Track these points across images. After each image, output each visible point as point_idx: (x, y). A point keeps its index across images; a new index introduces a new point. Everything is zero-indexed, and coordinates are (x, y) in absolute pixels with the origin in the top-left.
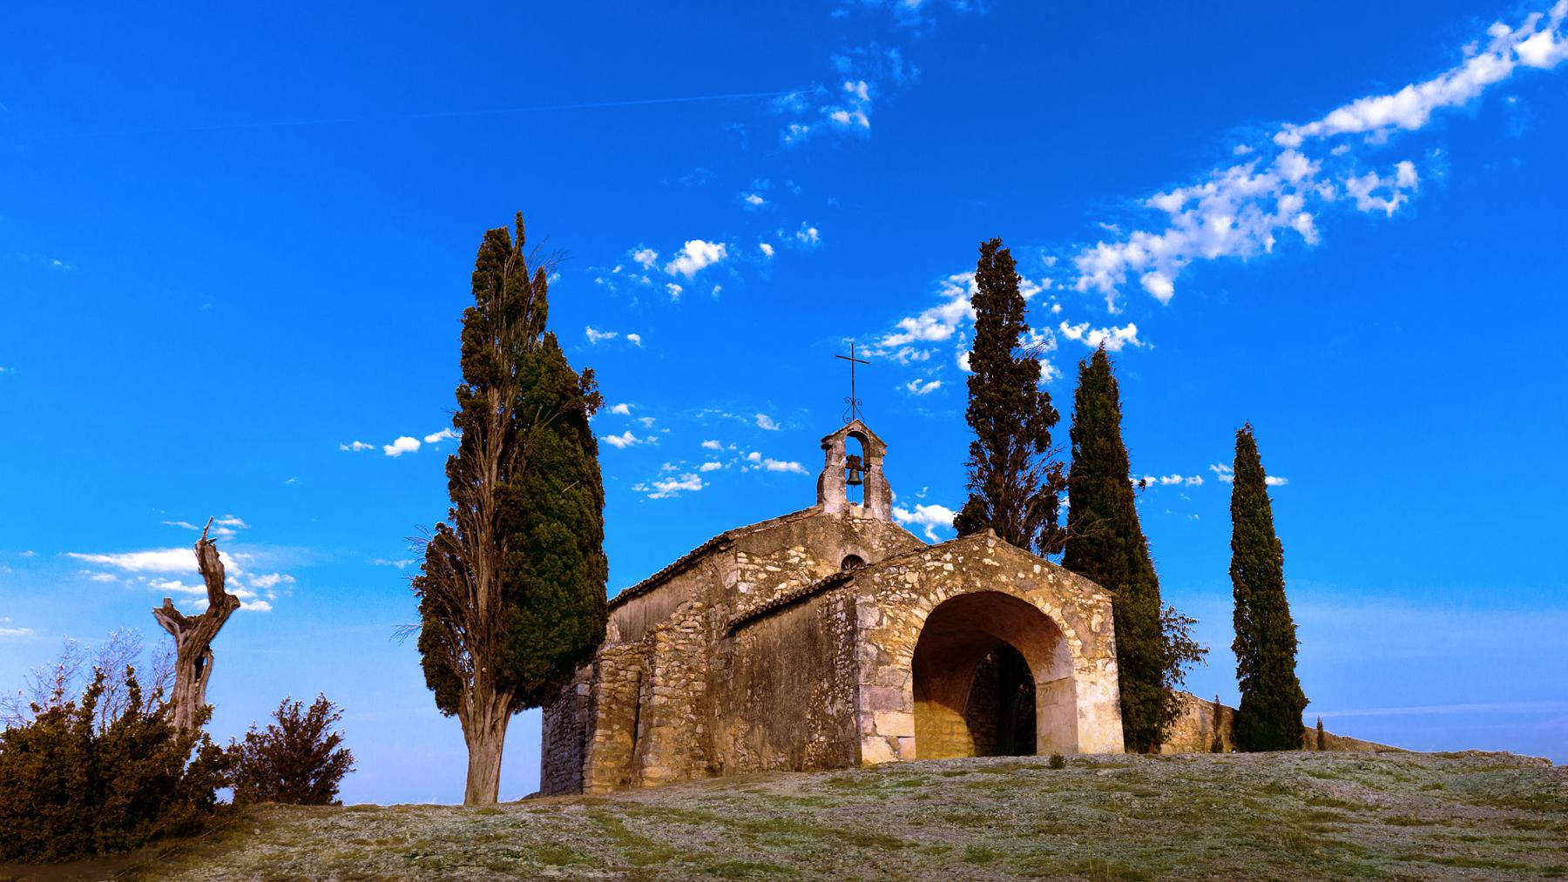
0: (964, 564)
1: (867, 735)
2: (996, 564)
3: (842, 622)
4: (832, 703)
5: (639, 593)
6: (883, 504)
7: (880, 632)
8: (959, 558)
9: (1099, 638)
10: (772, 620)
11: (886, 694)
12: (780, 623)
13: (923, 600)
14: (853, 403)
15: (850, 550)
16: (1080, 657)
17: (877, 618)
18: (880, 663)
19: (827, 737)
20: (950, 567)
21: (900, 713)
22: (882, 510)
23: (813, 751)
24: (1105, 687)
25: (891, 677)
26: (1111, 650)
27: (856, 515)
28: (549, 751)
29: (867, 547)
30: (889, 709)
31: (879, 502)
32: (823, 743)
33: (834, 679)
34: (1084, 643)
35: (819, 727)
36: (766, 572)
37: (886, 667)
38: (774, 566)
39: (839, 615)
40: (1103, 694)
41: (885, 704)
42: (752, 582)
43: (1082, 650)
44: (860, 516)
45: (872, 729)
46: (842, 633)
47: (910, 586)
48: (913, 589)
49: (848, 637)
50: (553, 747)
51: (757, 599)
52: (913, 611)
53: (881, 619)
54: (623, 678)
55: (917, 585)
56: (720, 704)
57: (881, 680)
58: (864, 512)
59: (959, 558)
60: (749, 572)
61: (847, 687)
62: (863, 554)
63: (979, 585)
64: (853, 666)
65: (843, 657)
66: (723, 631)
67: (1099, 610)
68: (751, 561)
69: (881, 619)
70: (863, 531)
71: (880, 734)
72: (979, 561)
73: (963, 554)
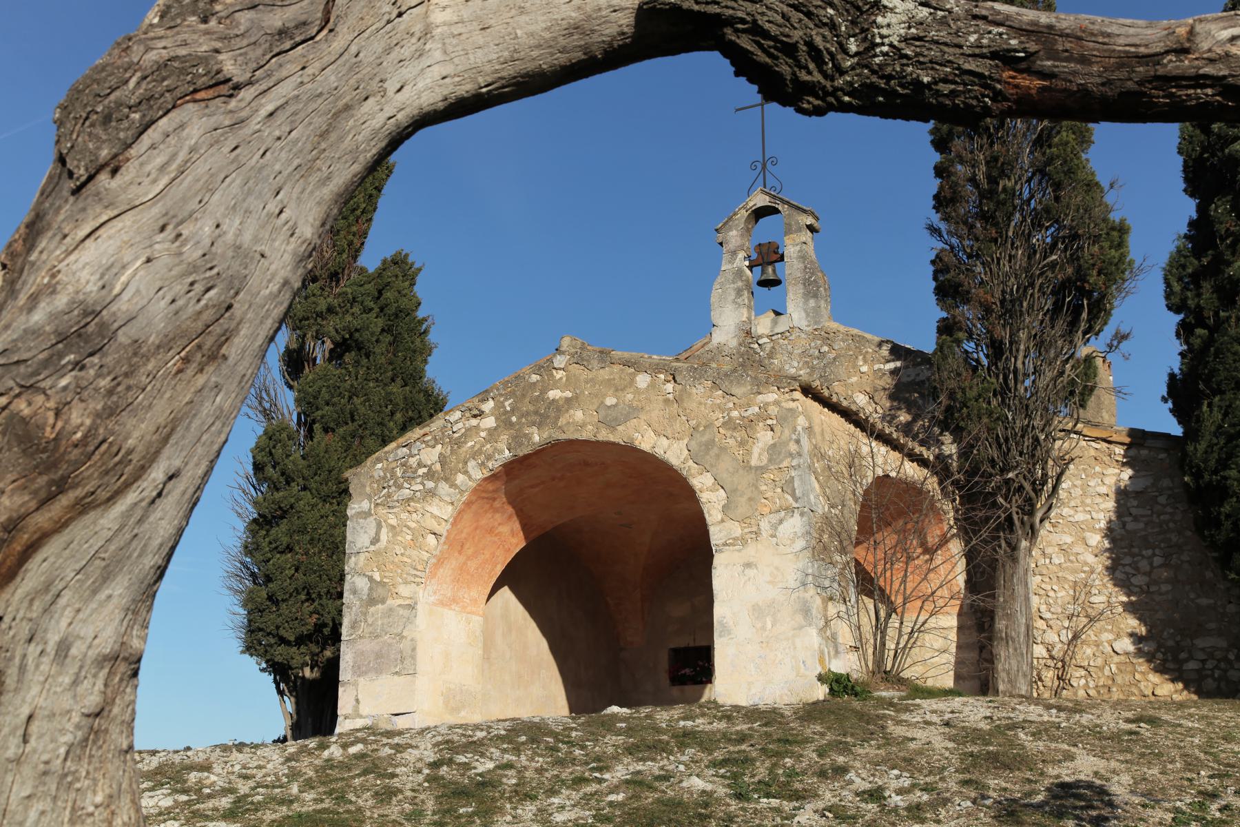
2: (569, 394)
6: (806, 301)
7: (377, 553)
8: (507, 404)
11: (377, 648)
13: (444, 488)
16: (723, 521)
17: (372, 533)
18: (372, 601)
21: (396, 677)
22: (805, 311)
24: (777, 568)
25: (386, 621)
30: (379, 671)
31: (800, 301)
34: (731, 494)
37: (380, 606)
40: (769, 582)
43: (725, 509)
47: (425, 470)
48: (430, 475)
52: (428, 508)
58: (775, 323)
59: (507, 404)
63: (536, 438)
67: (770, 422)
72: (542, 397)
73: (512, 394)
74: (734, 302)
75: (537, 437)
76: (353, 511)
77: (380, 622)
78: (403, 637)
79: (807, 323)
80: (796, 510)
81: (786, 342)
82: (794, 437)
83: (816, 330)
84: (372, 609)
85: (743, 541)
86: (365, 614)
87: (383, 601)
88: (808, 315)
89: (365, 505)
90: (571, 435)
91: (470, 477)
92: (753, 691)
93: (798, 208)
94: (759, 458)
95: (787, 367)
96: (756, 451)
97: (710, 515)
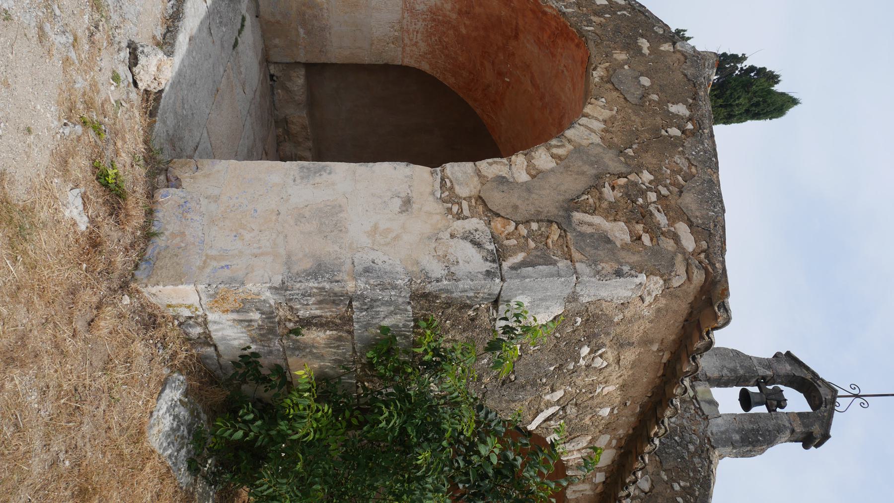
9: (555, 233)
14: (857, 396)
22: (727, 430)
24: (397, 238)
40: (375, 228)
67: (646, 239)
74: (723, 367)
79: (714, 432)
80: (495, 265)
81: (693, 412)
82: (626, 269)
83: (709, 439)
88: (722, 433)
92: (204, 202)
94: (581, 223)
97: (490, 164)
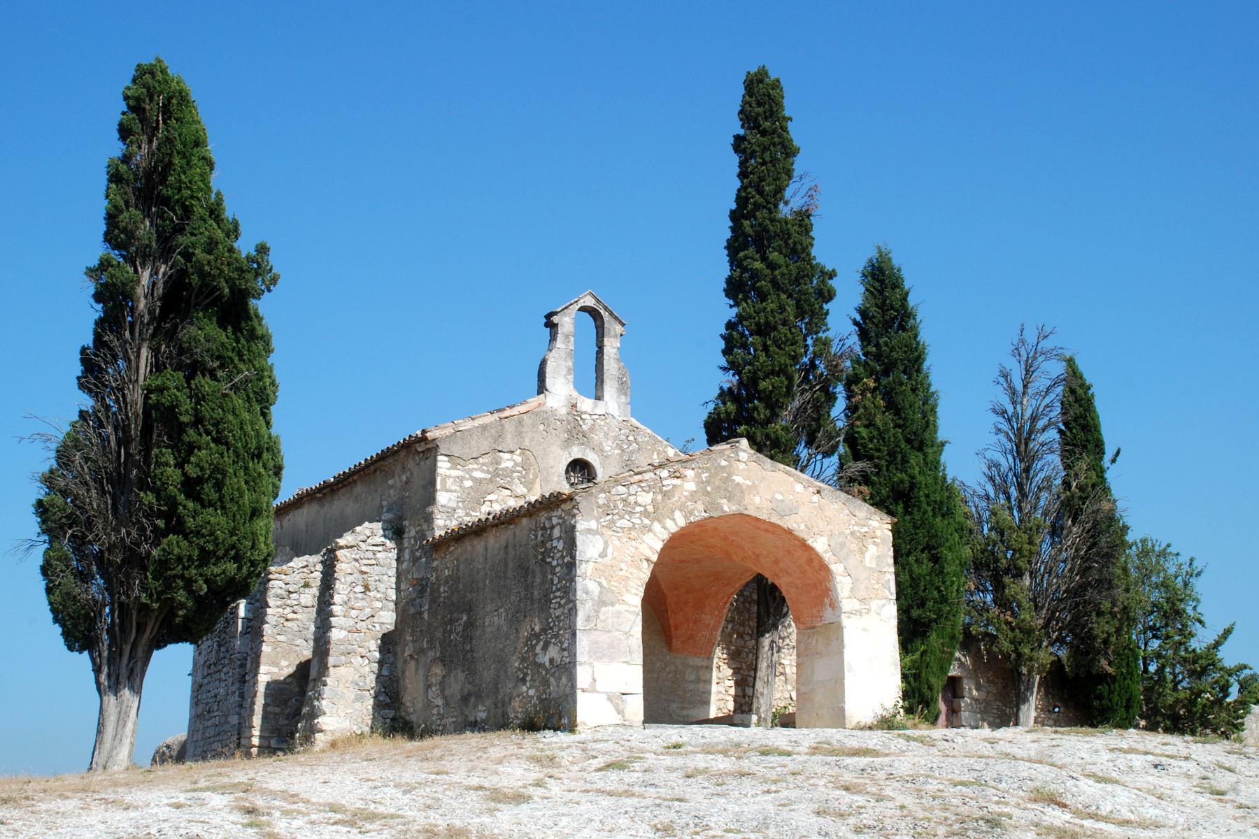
0: (708, 482)
1: (583, 691)
2: (748, 482)
3: (559, 551)
4: (545, 648)
5: (318, 495)
6: (618, 397)
8: (703, 476)
10: (475, 542)
12: (486, 548)
13: (657, 526)
15: (577, 453)
18: (602, 603)
19: (537, 690)
20: (691, 486)
23: (520, 707)
25: (615, 620)
26: (889, 590)
27: (584, 409)
28: (201, 686)
29: (600, 450)
32: (532, 697)
33: (547, 620)
34: (855, 581)
35: (528, 678)
36: (473, 479)
37: (610, 608)
38: (483, 471)
39: (555, 543)
41: (608, 653)
42: (455, 491)
44: (589, 411)
45: (591, 683)
46: (558, 565)
47: (642, 509)
48: (646, 514)
49: (565, 570)
50: (206, 681)
51: (460, 512)
53: (605, 549)
54: (295, 603)
55: (650, 508)
56: (413, 641)
57: (603, 624)
59: (703, 476)
60: (452, 480)
61: (561, 632)
62: (591, 457)
64: (571, 605)
65: (558, 594)
66: (417, 550)
68: (454, 467)
69: (605, 549)
70: (592, 429)
71: (600, 690)
73: (708, 470)
75: (728, 507)
76: (583, 527)
77: (610, 621)
78: (630, 635)
84: (603, 609)
85: (858, 613)
86: (597, 612)
87: (612, 604)
89: (593, 525)
90: (752, 512)
91: (676, 524)
93: (616, 318)
95: (604, 444)
96: (868, 555)
